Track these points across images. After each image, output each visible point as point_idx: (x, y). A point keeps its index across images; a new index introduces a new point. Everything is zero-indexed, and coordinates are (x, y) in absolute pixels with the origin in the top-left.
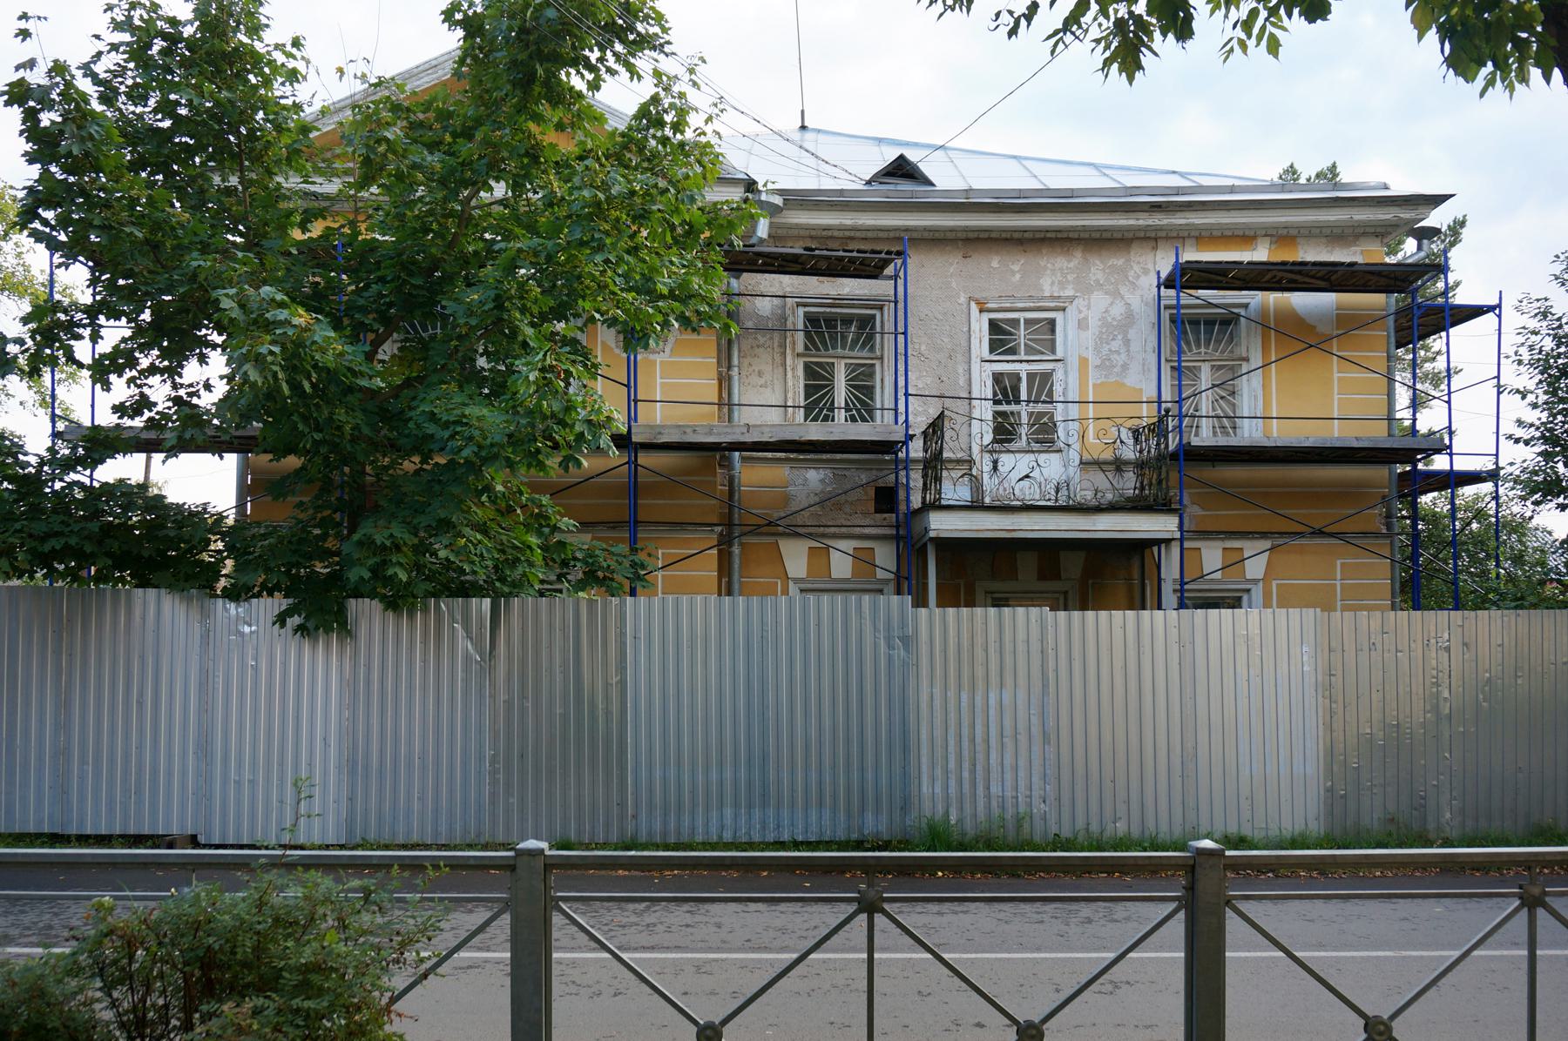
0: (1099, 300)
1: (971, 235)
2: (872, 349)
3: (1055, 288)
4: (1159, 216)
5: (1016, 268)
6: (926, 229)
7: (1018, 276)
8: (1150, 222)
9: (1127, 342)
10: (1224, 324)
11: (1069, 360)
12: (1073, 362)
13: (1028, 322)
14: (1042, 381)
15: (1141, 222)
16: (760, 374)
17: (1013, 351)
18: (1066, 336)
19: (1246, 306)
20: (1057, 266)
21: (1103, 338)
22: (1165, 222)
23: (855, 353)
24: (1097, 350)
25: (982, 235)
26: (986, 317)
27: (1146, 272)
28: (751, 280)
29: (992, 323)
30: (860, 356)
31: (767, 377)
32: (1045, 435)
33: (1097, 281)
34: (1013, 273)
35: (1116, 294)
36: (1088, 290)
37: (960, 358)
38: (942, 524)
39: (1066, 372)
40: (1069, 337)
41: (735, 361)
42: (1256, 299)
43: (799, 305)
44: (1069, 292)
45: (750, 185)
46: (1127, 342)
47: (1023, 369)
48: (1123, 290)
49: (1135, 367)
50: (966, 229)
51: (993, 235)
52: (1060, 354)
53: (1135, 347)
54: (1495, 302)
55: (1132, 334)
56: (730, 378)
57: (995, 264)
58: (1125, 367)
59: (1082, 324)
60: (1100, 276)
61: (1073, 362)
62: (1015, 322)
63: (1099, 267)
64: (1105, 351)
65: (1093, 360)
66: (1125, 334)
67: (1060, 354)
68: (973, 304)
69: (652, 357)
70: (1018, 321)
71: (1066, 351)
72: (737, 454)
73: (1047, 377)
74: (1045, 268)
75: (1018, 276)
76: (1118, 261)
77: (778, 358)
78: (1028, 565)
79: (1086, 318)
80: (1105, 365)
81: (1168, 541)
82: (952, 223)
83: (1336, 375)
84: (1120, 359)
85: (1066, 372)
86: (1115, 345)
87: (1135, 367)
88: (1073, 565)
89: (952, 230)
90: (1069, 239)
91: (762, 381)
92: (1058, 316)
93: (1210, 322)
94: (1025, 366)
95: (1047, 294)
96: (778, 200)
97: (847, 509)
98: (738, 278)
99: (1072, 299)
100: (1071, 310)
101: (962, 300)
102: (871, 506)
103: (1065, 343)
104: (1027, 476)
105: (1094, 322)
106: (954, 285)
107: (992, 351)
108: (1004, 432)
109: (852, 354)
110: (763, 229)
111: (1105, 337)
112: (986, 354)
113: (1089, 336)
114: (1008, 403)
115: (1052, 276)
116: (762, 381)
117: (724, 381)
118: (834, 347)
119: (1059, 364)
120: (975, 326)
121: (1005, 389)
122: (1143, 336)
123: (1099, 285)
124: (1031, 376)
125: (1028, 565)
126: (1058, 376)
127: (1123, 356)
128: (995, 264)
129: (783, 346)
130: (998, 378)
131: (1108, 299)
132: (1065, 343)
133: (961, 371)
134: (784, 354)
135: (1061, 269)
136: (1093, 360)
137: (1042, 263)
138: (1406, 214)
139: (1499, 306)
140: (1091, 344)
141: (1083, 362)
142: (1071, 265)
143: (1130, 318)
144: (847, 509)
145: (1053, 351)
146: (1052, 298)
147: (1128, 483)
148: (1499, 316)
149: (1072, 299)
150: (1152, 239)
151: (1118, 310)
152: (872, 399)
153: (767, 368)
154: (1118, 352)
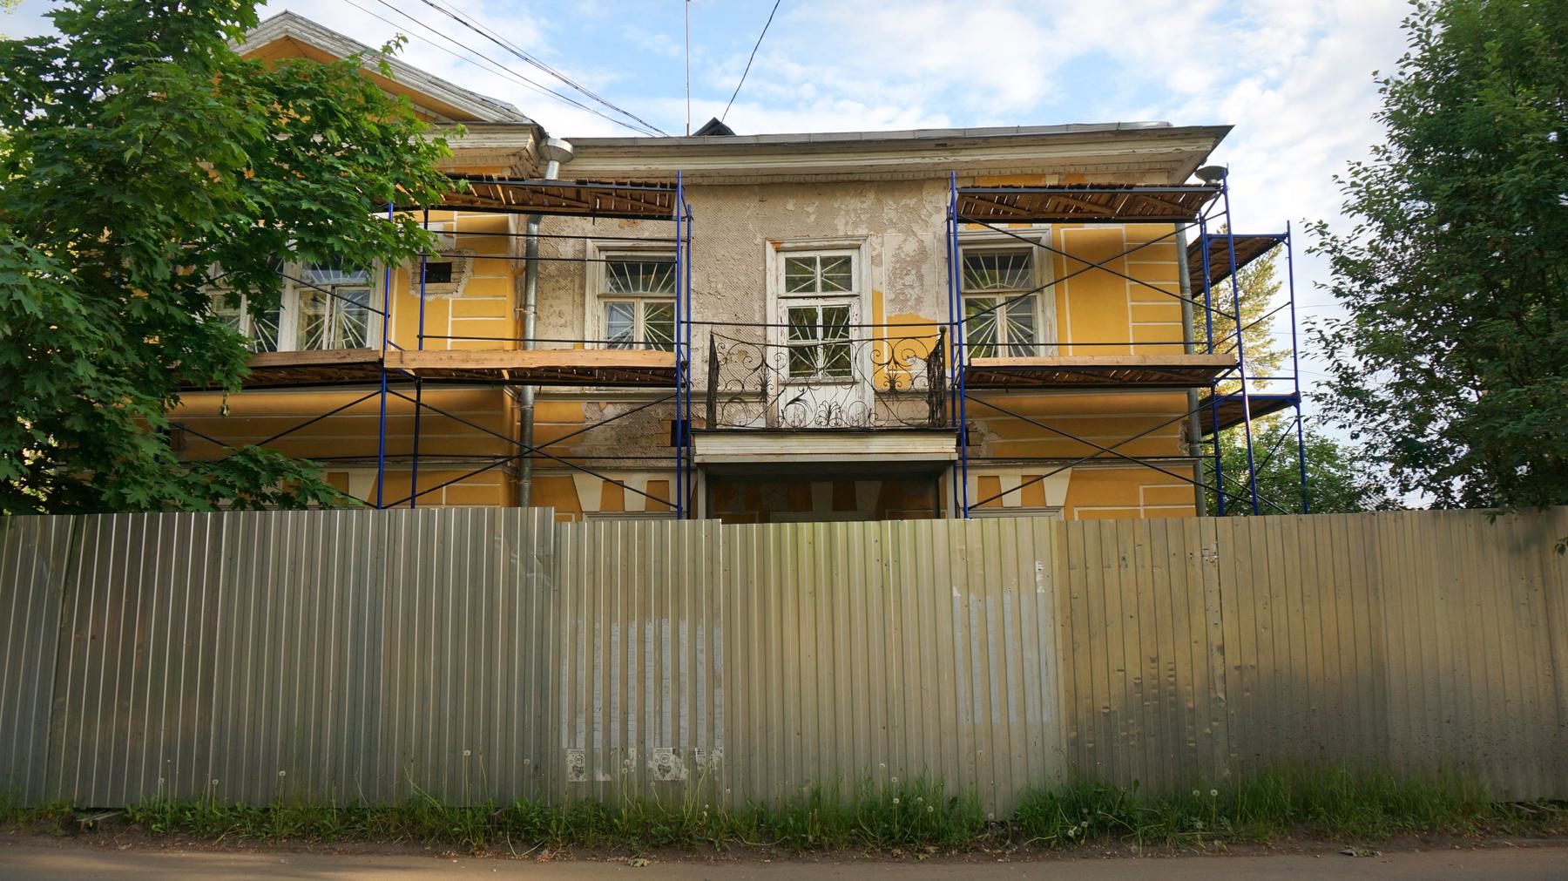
0: (893, 238)
1: (765, 179)
4: (947, 154)
5: (810, 209)
6: (718, 172)
7: (812, 218)
8: (936, 160)
9: (920, 277)
10: (1015, 261)
12: (867, 296)
13: (825, 262)
14: (838, 320)
15: (927, 160)
16: (560, 315)
17: (811, 288)
19: (1037, 241)
21: (896, 274)
22: (951, 159)
23: (657, 293)
24: (891, 284)
25: (776, 180)
26: (782, 257)
27: (938, 210)
28: (548, 223)
29: (790, 264)
30: (661, 295)
31: (568, 317)
32: (840, 366)
33: (890, 220)
34: (809, 215)
35: (909, 232)
36: (880, 228)
37: (756, 294)
38: (708, 449)
41: (532, 301)
42: (1044, 231)
43: (601, 249)
44: (862, 231)
45: (540, 134)
46: (920, 277)
47: (819, 305)
48: (916, 228)
49: (929, 300)
50: (759, 173)
51: (787, 179)
52: (855, 290)
53: (927, 281)
54: (1283, 231)
55: (925, 268)
57: (791, 206)
58: (919, 300)
59: (876, 261)
60: (893, 215)
61: (867, 296)
62: (811, 262)
63: (891, 208)
64: (899, 286)
66: (919, 269)
67: (855, 290)
68: (769, 245)
69: (445, 297)
73: (844, 312)
75: (812, 218)
76: (911, 201)
78: (822, 492)
79: (880, 255)
80: (900, 299)
81: (953, 462)
83: (1130, 304)
84: (913, 293)
86: (909, 280)
87: (929, 300)
88: (868, 492)
89: (746, 174)
91: (562, 321)
92: (853, 254)
94: (821, 302)
95: (841, 233)
96: (568, 147)
98: (537, 222)
99: (865, 238)
101: (759, 241)
104: (797, 399)
105: (887, 258)
107: (788, 290)
108: (800, 361)
109: (648, 293)
110: (553, 172)
111: (898, 267)
112: (783, 291)
113: (882, 273)
114: (806, 337)
115: (844, 219)
116: (562, 321)
117: (521, 321)
118: (636, 289)
119: (855, 300)
120: (770, 264)
121: (800, 321)
122: (935, 272)
123: (892, 224)
124: (828, 313)
125: (822, 492)
126: (854, 311)
130: (793, 313)
131: (901, 237)
133: (756, 307)
134: (583, 295)
136: (887, 294)
138: (1188, 148)
139: (1288, 235)
140: (885, 279)
141: (877, 296)
143: (923, 254)
144: (644, 442)
145: (850, 289)
146: (847, 237)
147: (920, 411)
148: (1289, 245)
149: (865, 238)
150: (940, 179)
151: (911, 247)
152: (672, 336)
153: (567, 309)
154: (911, 287)
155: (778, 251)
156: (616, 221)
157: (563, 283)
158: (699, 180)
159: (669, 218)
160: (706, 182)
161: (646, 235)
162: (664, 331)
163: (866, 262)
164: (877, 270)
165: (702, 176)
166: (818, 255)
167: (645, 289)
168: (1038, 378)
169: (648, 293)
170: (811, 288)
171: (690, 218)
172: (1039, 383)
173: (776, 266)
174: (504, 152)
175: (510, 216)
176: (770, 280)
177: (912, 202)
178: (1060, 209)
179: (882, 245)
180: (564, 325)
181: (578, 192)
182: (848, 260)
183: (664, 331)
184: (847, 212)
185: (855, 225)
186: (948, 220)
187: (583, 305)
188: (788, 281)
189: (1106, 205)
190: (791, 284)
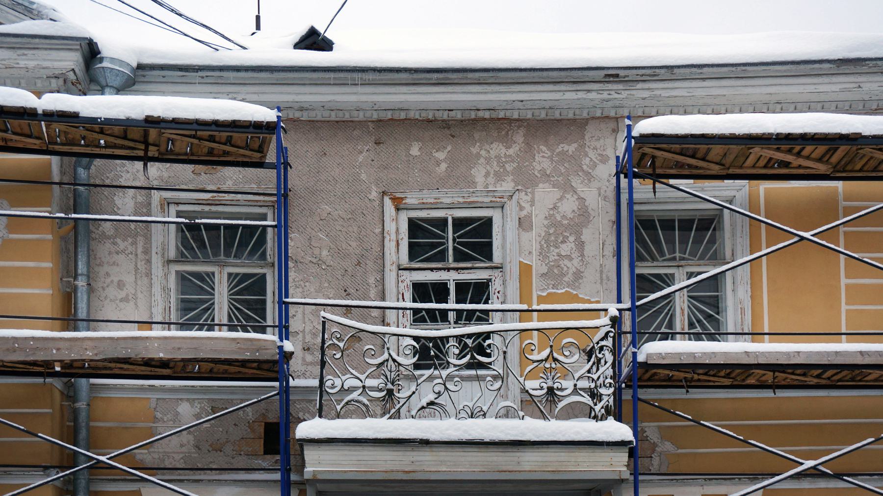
0: (545, 195)
2: (263, 256)
3: (491, 180)
5: (441, 155)
7: (444, 166)
8: (605, 95)
11: (507, 268)
13: (459, 223)
16: (121, 285)
17: (441, 256)
18: (504, 238)
20: (493, 153)
21: (550, 241)
24: (543, 254)
27: (604, 160)
29: (415, 227)
31: (129, 289)
33: (543, 172)
34: (438, 164)
35: (567, 188)
36: (527, 181)
37: (370, 264)
39: (504, 282)
40: (505, 240)
41: (82, 268)
44: (507, 186)
47: (451, 278)
48: (576, 182)
51: (411, 115)
53: (591, 249)
55: (587, 235)
56: (75, 289)
57: (415, 151)
58: (578, 275)
59: (524, 224)
60: (546, 165)
64: (553, 257)
65: (538, 267)
70: (445, 220)
71: (504, 257)
72: (83, 381)
74: (478, 156)
75: (444, 166)
77: (141, 265)
79: (529, 216)
80: (554, 274)
82: (353, 98)
83: (844, 281)
85: (504, 282)
86: (565, 249)
87: (590, 275)
90: (509, 121)
93: (686, 224)
97: (228, 449)
100: (511, 207)
101: (374, 195)
102: (260, 445)
103: (503, 246)
105: (539, 221)
106: (363, 176)
113: (533, 239)
116: (122, 294)
118: (216, 254)
119: (496, 273)
120: (390, 226)
122: (599, 237)
123: (546, 177)
124: (462, 288)
127: (576, 262)
128: (415, 151)
129: (147, 251)
131: (556, 193)
132: (503, 246)
133: (372, 281)
134: (149, 261)
135: (498, 157)
136: (538, 267)
137: (474, 150)
140: (535, 248)
141: (525, 270)
142: (511, 152)
143: (584, 215)
145: (490, 257)
151: (569, 206)
154: (569, 258)
155: (398, 209)
156: (189, 167)
157: (122, 245)
158: (298, 114)
159: (260, 165)
160: (305, 116)
161: (228, 185)
162: (250, 304)
163: (512, 224)
164: (525, 236)
165: (301, 109)
166: (450, 215)
167: (227, 255)
168: (727, 376)
169: (231, 260)
170: (441, 256)
171: (287, 165)
172: (727, 382)
173: (397, 228)
174: (44, 73)
175: (55, 160)
176: (390, 246)
177: (571, 148)
178: (762, 163)
179: (532, 203)
180: (125, 299)
181: (146, 134)
182: (489, 222)
183: (250, 304)
184: (488, 160)
185: (499, 177)
186: (617, 175)
187: (149, 274)
188: (411, 246)
189: (820, 160)
190: (415, 252)
